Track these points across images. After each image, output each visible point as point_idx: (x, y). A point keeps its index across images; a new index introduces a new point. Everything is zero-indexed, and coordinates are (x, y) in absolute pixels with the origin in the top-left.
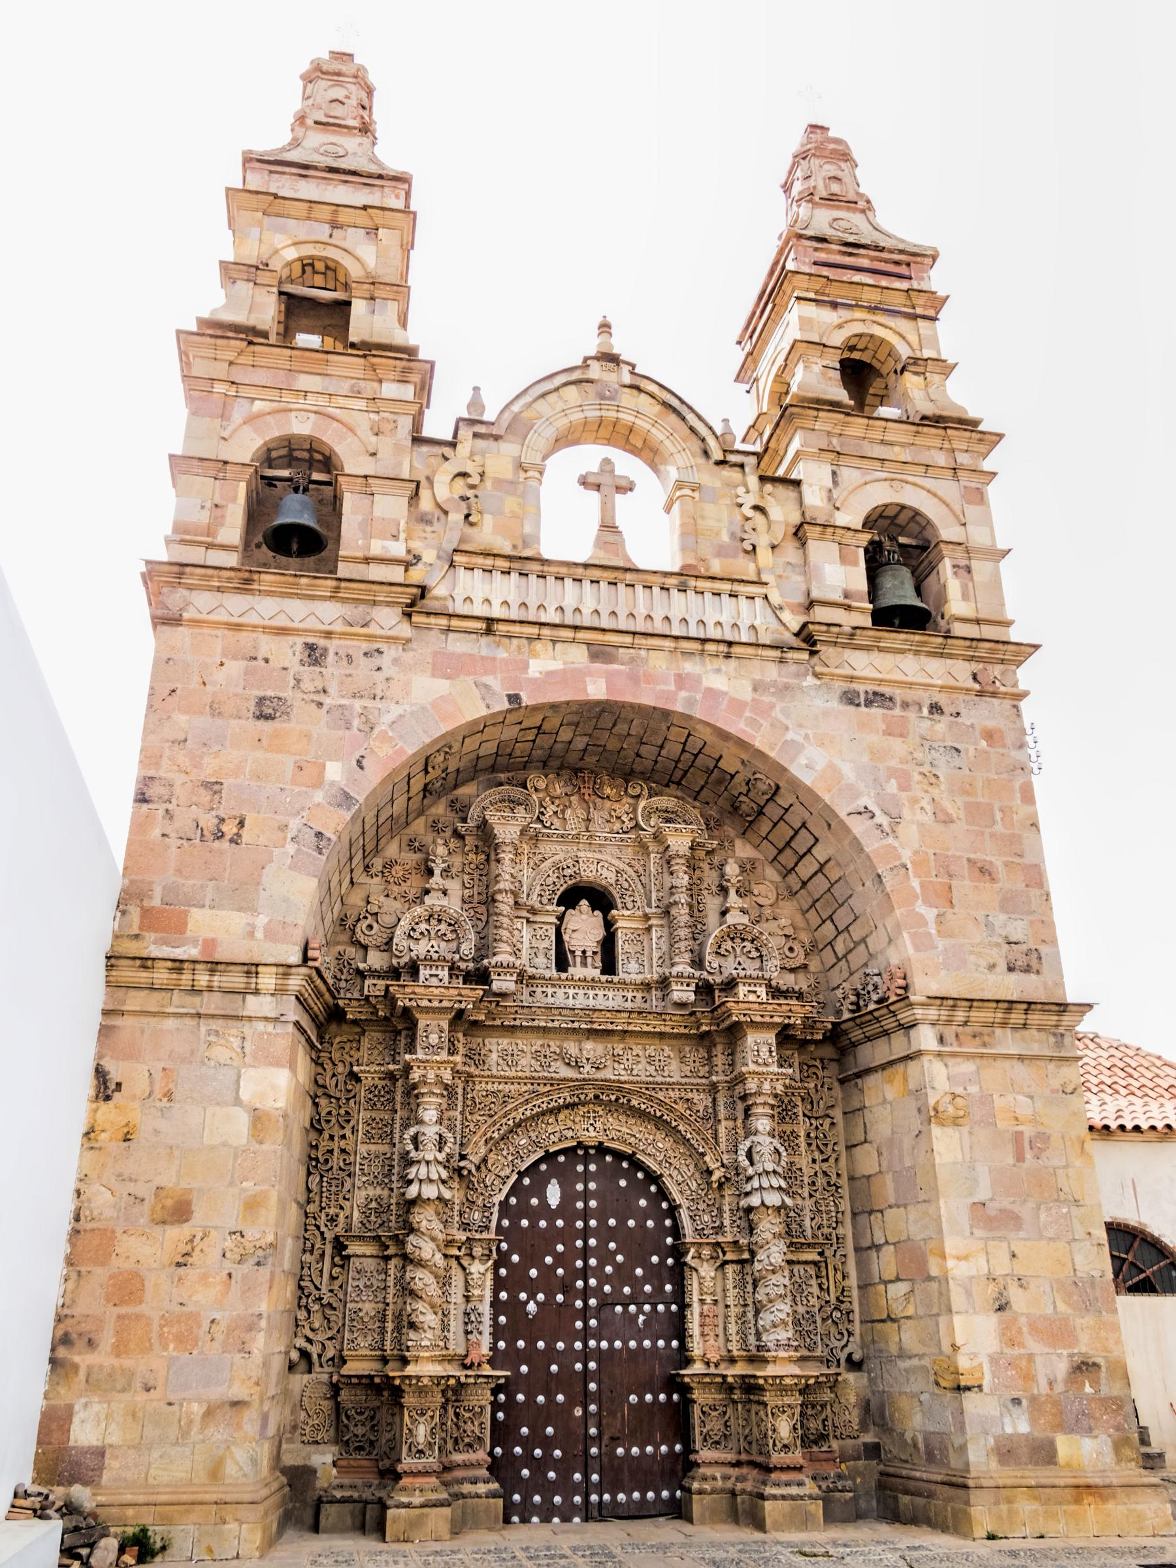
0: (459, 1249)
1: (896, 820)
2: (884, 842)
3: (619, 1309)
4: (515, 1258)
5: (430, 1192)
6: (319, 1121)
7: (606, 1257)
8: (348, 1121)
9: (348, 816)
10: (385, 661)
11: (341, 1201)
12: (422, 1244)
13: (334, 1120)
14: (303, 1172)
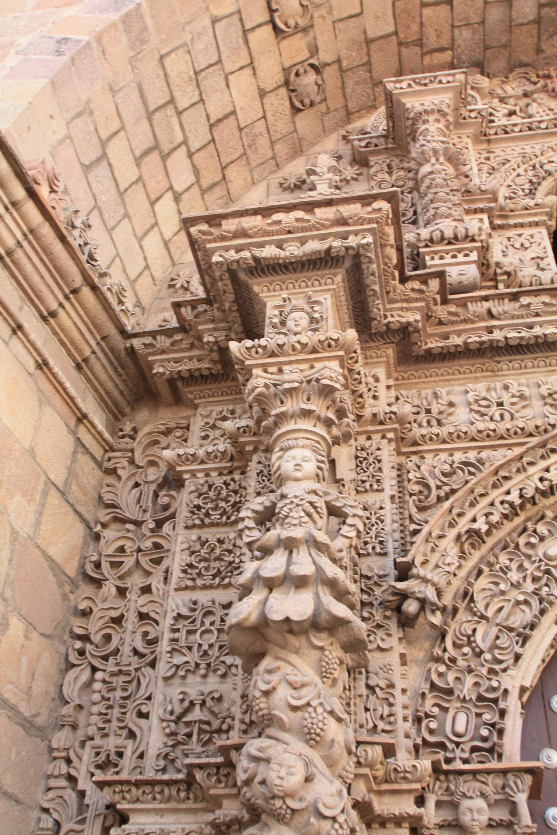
0: (420, 801)
5: (295, 606)
6: (98, 565)
8: (157, 562)
11: (131, 720)
12: (274, 750)
13: (129, 562)
14: (48, 663)
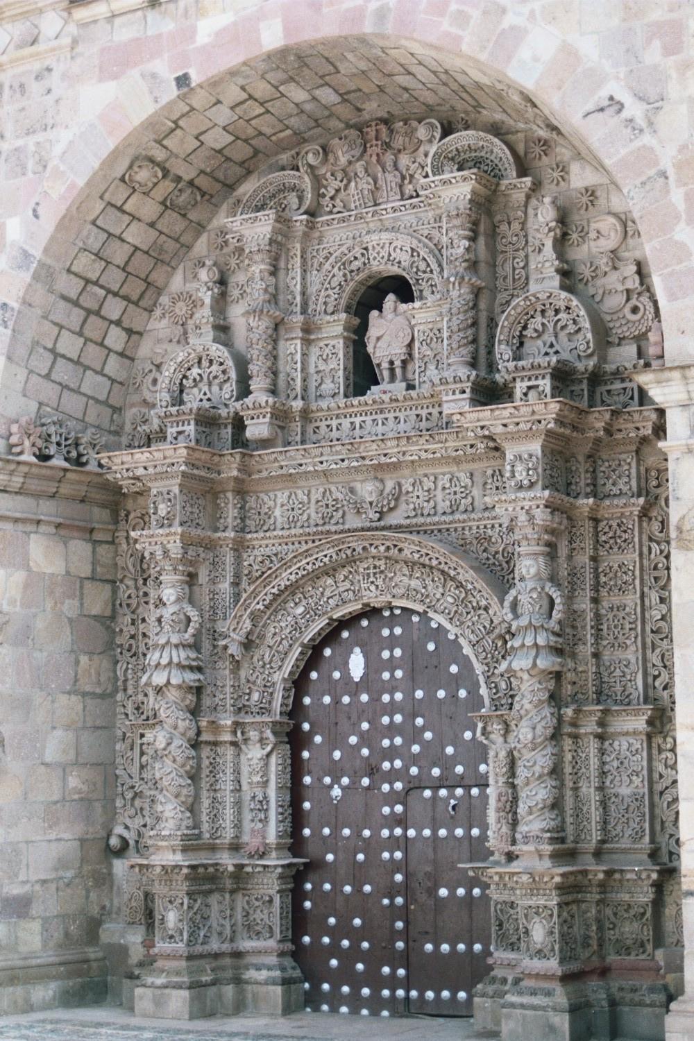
1: (655, 103)
2: (637, 143)
3: (428, 793)
4: (318, 739)
7: (414, 735)
9: (27, 277)
10: (54, 80)
